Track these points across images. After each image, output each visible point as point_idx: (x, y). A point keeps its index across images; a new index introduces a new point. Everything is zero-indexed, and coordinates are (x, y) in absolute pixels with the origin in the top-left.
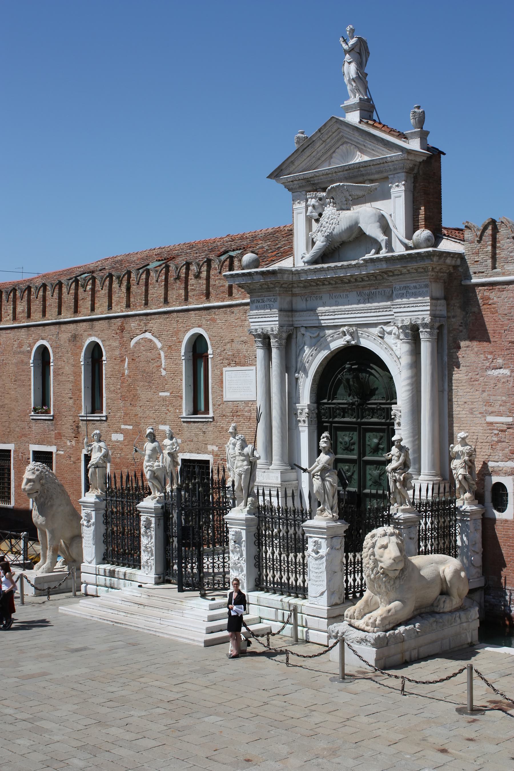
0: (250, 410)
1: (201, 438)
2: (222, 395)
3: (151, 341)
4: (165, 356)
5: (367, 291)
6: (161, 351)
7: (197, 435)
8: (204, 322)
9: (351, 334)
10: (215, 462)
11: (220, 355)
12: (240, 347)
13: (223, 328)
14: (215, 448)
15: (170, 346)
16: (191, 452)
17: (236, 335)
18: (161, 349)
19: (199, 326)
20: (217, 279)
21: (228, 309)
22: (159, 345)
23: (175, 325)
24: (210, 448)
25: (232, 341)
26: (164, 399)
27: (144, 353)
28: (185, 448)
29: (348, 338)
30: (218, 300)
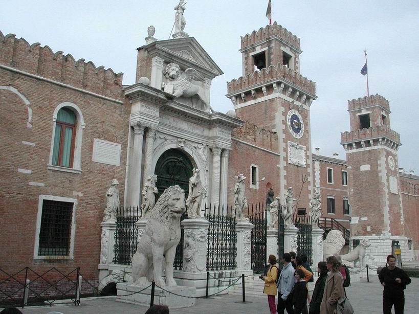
0: (114, 172)
1: (67, 184)
2: (91, 157)
3: (16, 95)
4: (33, 114)
5: (192, 125)
6: (28, 108)
7: (62, 182)
8: (79, 101)
9: (184, 143)
10: (79, 204)
11: (92, 129)
12: (109, 128)
13: (97, 111)
14: (81, 194)
15: (40, 107)
16: (54, 194)
17: (107, 119)
18: (30, 106)
19: (74, 103)
20: (94, 78)
21: (102, 101)
22: (27, 102)
23: (48, 92)
24: (75, 193)
25: (104, 122)
26: (28, 148)
27: (6, 102)
28: (49, 191)
29: (182, 144)
30: (93, 90)
